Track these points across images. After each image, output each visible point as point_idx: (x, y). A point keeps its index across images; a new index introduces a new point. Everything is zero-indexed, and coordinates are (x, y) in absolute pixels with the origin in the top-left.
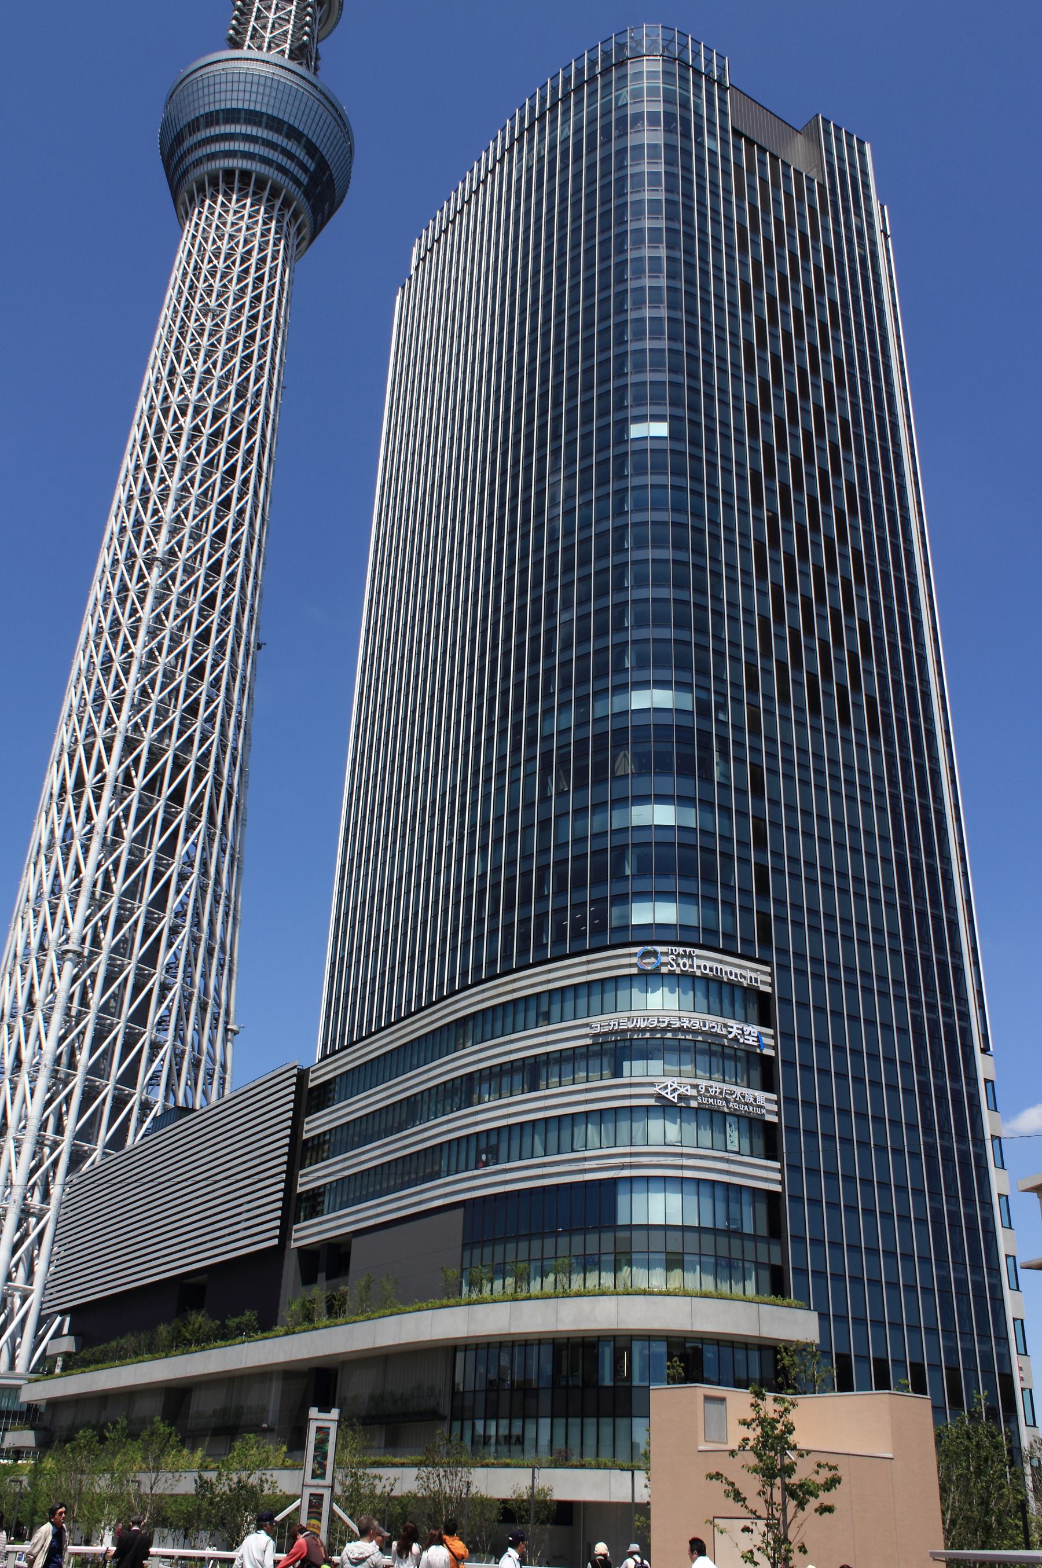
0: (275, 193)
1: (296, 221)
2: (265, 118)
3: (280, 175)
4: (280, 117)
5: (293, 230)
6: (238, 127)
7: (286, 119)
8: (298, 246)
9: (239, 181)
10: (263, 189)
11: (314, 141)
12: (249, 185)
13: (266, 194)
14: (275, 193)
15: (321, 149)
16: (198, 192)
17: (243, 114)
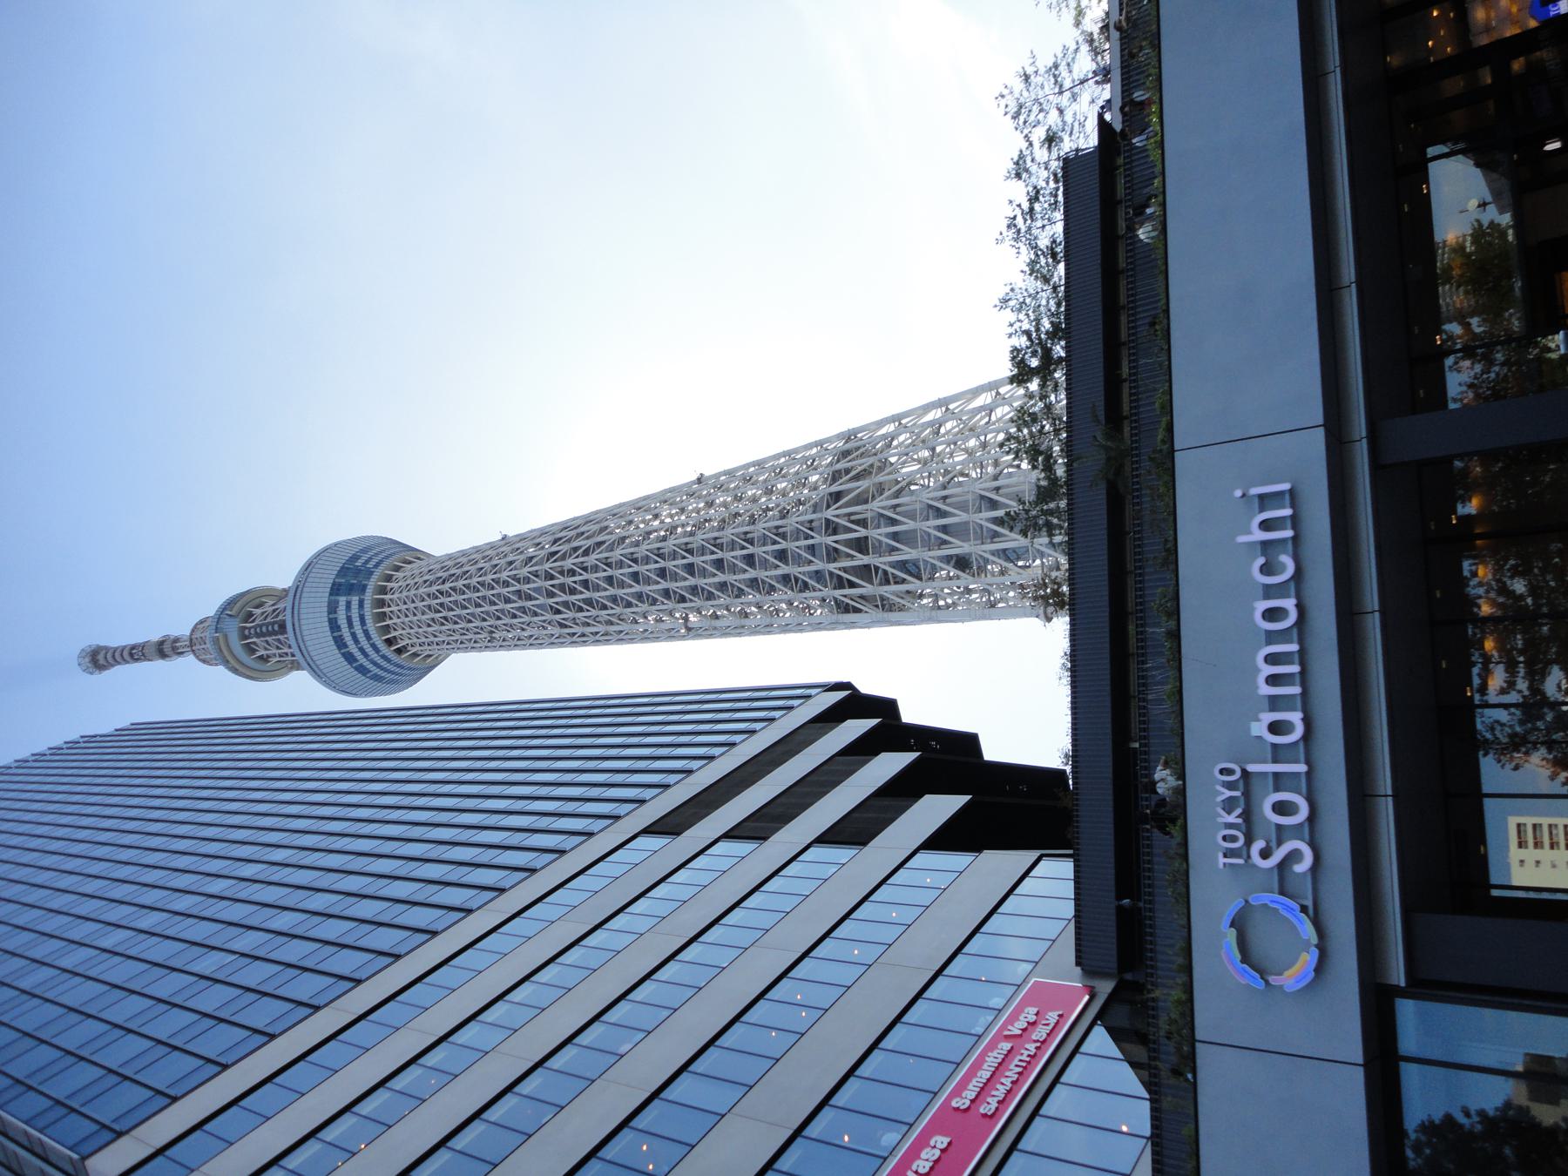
0: (383, 590)
1: (402, 567)
2: (331, 616)
3: (367, 590)
4: (326, 604)
5: (409, 566)
6: (345, 635)
7: (327, 599)
8: (419, 559)
9: (385, 621)
10: (383, 600)
11: (336, 572)
12: (385, 613)
13: (387, 597)
14: (383, 590)
15: (341, 565)
16: (409, 651)
17: (335, 634)
